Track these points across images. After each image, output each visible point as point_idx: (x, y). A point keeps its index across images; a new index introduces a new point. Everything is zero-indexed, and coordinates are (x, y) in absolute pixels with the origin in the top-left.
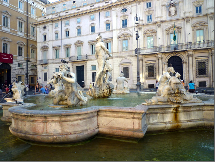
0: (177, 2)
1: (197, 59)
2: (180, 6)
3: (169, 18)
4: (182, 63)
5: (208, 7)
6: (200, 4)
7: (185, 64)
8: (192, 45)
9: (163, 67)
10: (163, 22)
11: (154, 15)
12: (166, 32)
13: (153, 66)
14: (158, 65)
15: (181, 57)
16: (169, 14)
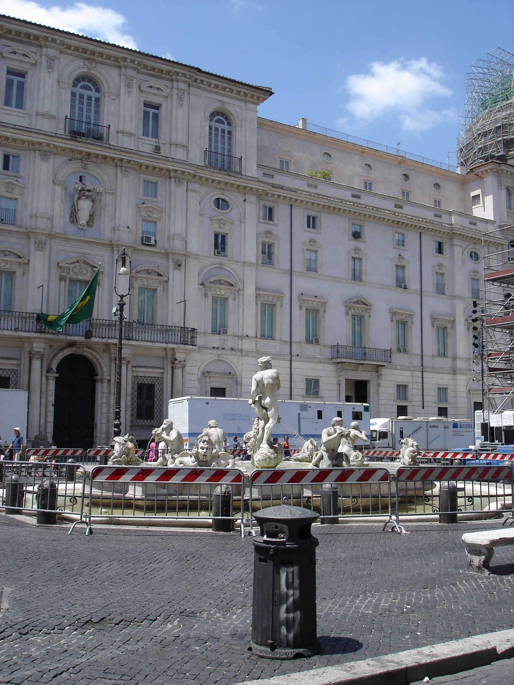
0: (102, 189)
1: (135, 374)
2: (103, 202)
3: (71, 229)
4: (95, 381)
5: (172, 232)
6: (155, 216)
7: (105, 384)
8: (134, 333)
9: (44, 386)
10: (52, 236)
11: (26, 205)
12: (59, 271)
13: (9, 378)
14: (26, 378)
15: (95, 361)
16: (71, 216)
